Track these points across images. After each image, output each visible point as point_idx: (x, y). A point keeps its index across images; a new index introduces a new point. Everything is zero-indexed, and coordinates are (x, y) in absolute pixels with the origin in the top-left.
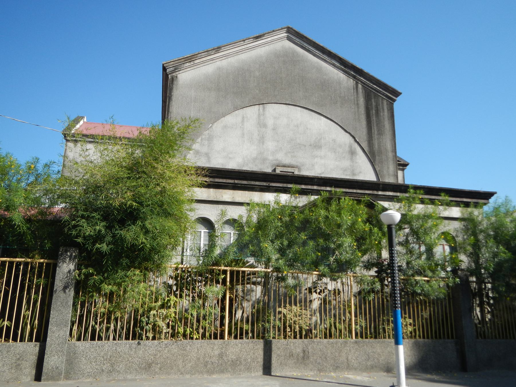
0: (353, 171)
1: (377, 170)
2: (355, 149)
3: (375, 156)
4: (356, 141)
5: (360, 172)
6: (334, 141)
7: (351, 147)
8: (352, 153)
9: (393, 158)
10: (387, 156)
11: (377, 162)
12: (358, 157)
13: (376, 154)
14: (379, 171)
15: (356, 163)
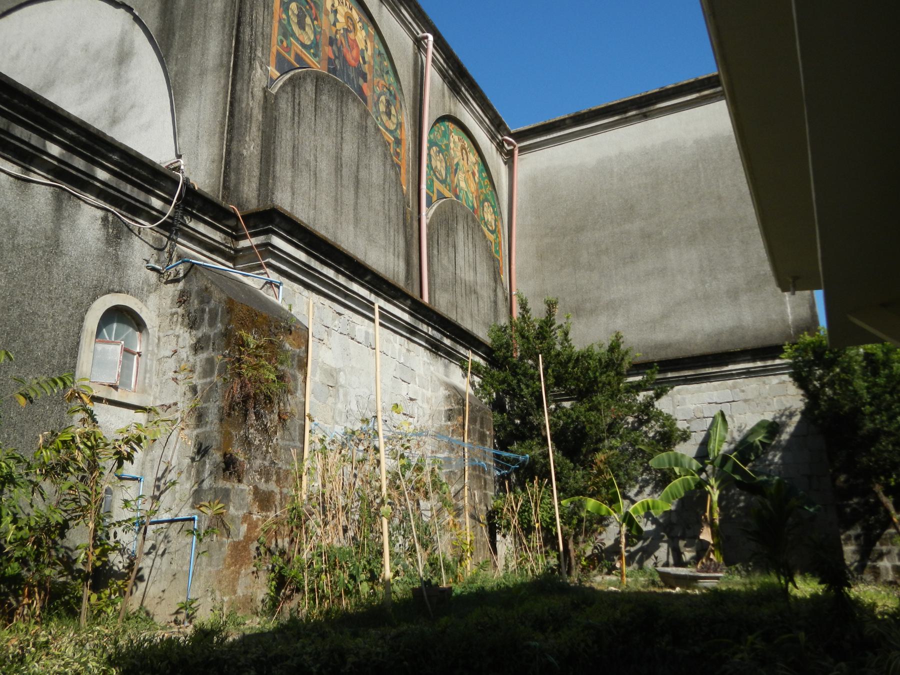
0: (115, 111)
1: (172, 75)
2: (132, 42)
3: (174, 34)
4: (137, 19)
5: (132, 107)
6: (86, 48)
7: (122, 40)
8: (123, 57)
9: (225, 12)
10: (205, 16)
11: (174, 51)
12: (135, 61)
13: (178, 24)
14: (176, 75)
15: (127, 82)
